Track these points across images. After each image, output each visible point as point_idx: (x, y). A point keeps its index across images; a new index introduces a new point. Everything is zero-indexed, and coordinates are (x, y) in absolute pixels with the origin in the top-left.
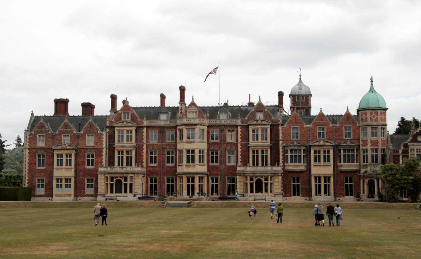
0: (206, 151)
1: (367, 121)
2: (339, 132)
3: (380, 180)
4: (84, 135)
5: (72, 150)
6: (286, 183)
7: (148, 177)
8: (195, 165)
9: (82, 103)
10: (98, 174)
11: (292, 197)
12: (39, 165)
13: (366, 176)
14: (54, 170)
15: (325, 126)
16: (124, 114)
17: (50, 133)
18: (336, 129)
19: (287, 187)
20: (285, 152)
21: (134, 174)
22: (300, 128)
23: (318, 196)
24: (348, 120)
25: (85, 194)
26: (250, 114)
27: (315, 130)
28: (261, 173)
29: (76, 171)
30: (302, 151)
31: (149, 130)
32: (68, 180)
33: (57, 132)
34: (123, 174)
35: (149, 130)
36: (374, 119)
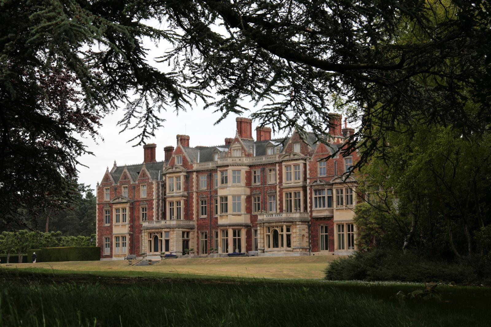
0: (243, 198)
4: (138, 186)
5: (126, 204)
6: (314, 234)
7: (199, 232)
8: (227, 215)
9: (165, 147)
10: (142, 230)
12: (106, 223)
14: (113, 226)
16: (178, 157)
17: (113, 185)
20: (311, 193)
21: (170, 228)
23: (341, 250)
25: (140, 253)
26: (288, 147)
28: (276, 222)
29: (132, 227)
30: (326, 190)
31: (199, 175)
32: (124, 238)
33: (119, 184)
34: (158, 229)
35: (199, 175)
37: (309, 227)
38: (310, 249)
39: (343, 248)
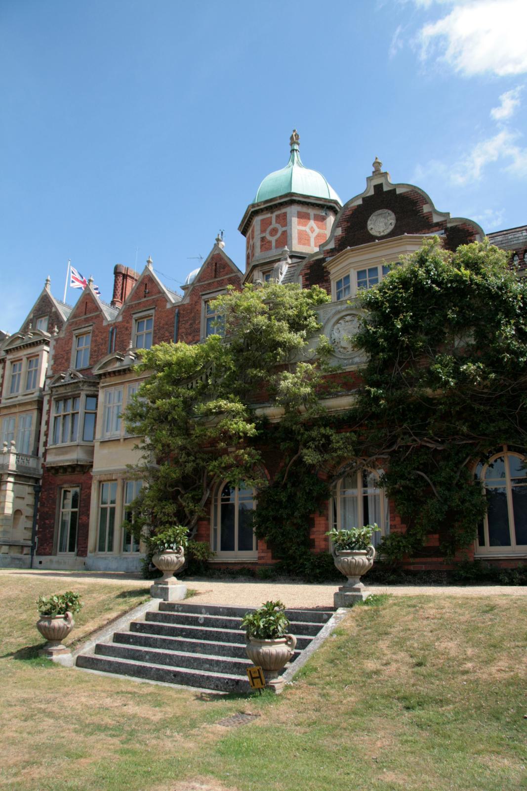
2: (190, 322)
11: (55, 554)
15: (152, 311)
18: (182, 312)
19: (47, 522)
22: (94, 331)
23: (106, 554)
24: (215, 277)
27: (127, 329)
36: (273, 239)
37: (37, 491)
38: (33, 548)
39: (111, 549)
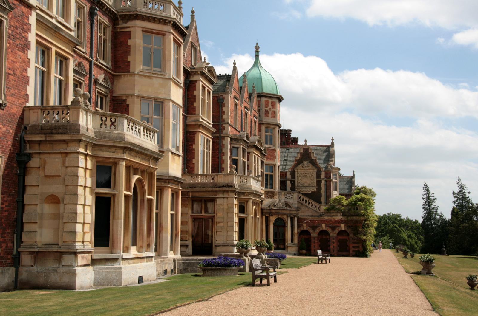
1: (274, 117)
3: (296, 220)
13: (274, 211)
